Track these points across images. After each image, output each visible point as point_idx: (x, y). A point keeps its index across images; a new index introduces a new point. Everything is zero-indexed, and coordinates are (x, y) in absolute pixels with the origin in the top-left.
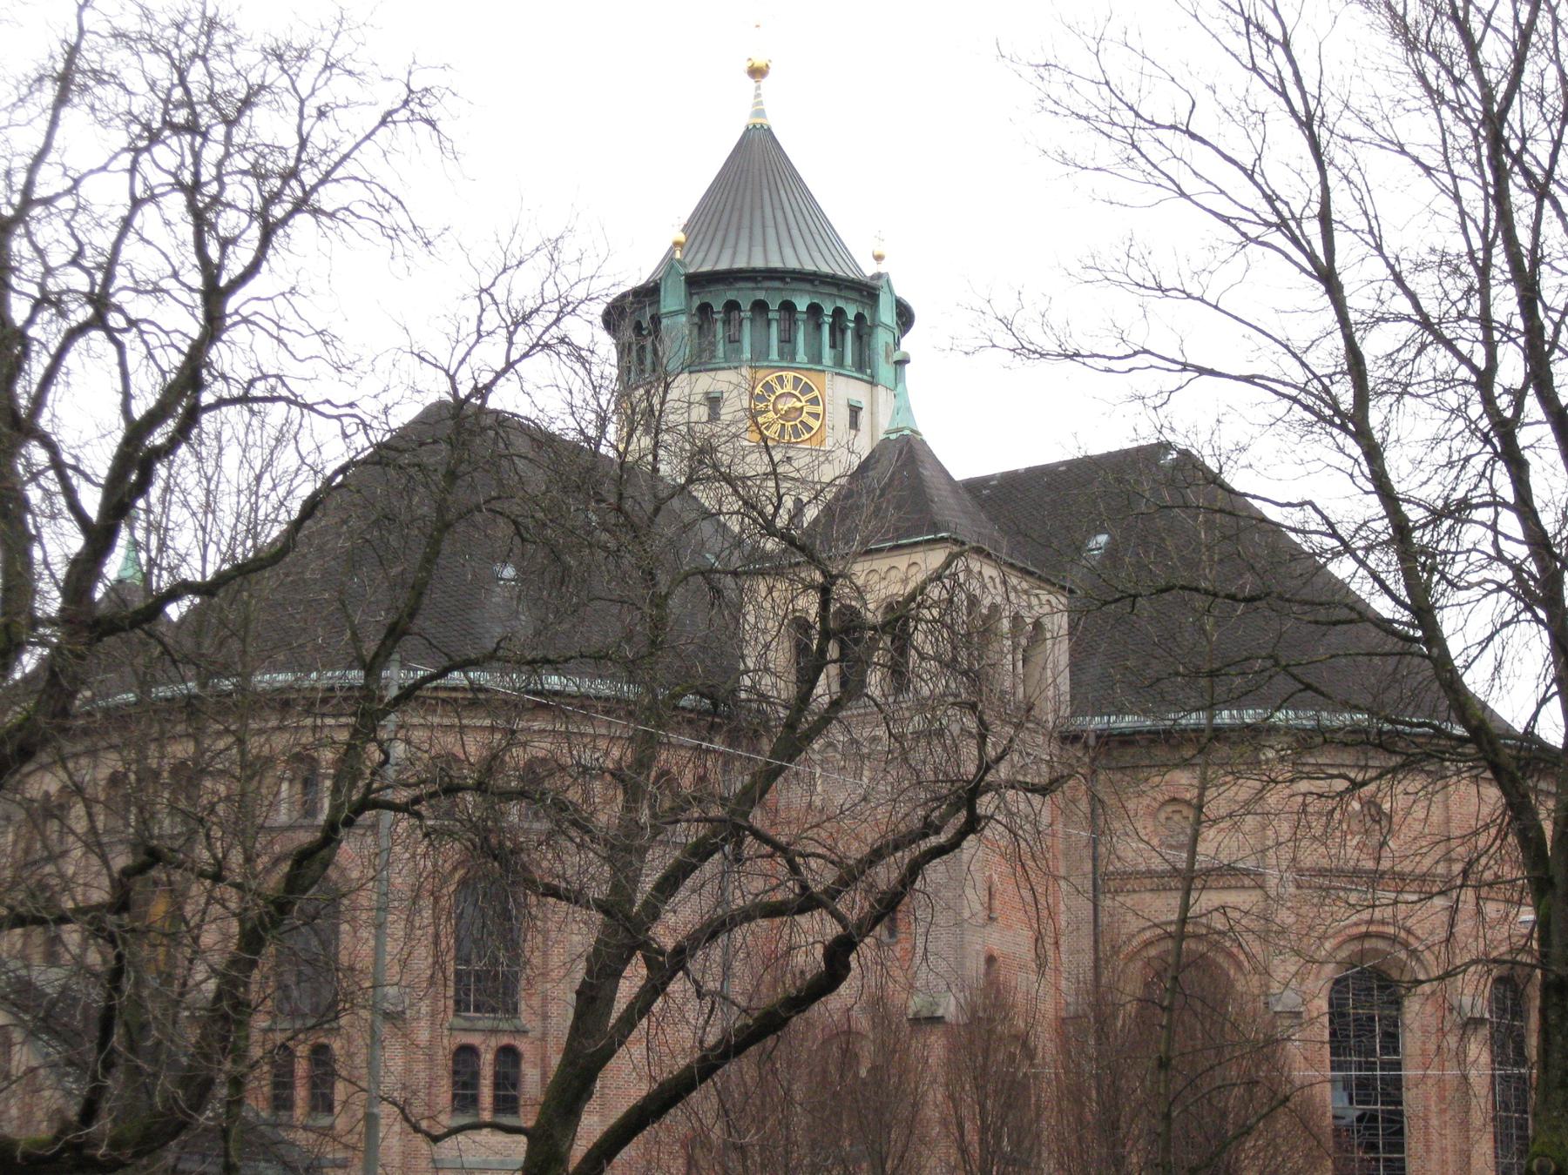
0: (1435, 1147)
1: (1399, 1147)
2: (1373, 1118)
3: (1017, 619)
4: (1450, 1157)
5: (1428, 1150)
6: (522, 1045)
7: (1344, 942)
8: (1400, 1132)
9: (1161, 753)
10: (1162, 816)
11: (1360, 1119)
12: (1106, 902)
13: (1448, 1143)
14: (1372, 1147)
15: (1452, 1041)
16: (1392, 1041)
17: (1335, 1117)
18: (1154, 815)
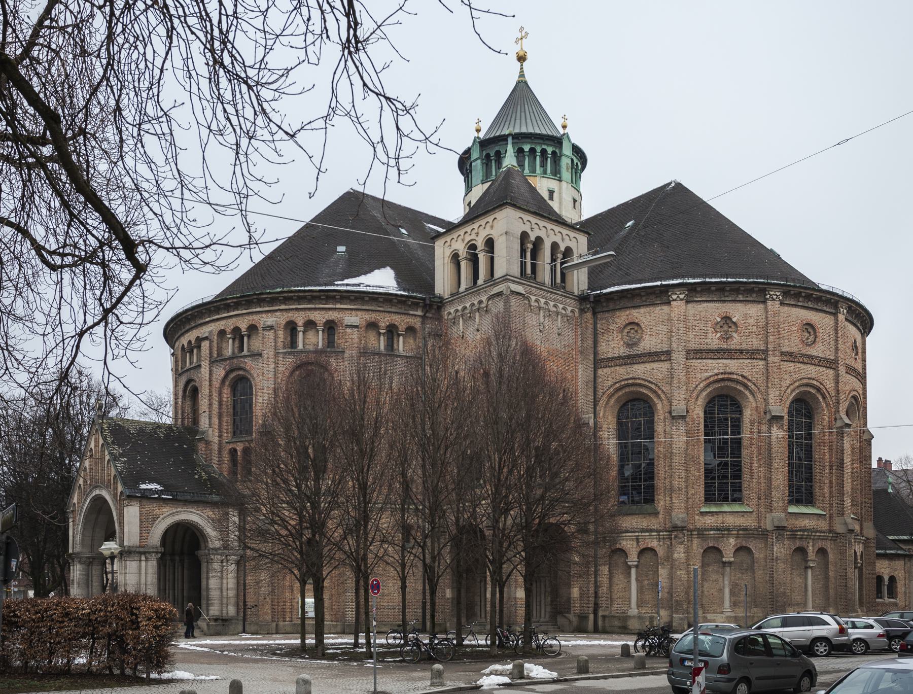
0: (756, 476)
1: (739, 477)
2: (726, 464)
3: (555, 246)
4: (762, 481)
5: (752, 478)
7: (710, 383)
8: (740, 470)
9: (623, 303)
10: (626, 331)
11: (719, 465)
12: (600, 372)
13: (761, 474)
14: (726, 477)
15: (764, 428)
16: (737, 429)
17: (705, 464)
18: (621, 330)
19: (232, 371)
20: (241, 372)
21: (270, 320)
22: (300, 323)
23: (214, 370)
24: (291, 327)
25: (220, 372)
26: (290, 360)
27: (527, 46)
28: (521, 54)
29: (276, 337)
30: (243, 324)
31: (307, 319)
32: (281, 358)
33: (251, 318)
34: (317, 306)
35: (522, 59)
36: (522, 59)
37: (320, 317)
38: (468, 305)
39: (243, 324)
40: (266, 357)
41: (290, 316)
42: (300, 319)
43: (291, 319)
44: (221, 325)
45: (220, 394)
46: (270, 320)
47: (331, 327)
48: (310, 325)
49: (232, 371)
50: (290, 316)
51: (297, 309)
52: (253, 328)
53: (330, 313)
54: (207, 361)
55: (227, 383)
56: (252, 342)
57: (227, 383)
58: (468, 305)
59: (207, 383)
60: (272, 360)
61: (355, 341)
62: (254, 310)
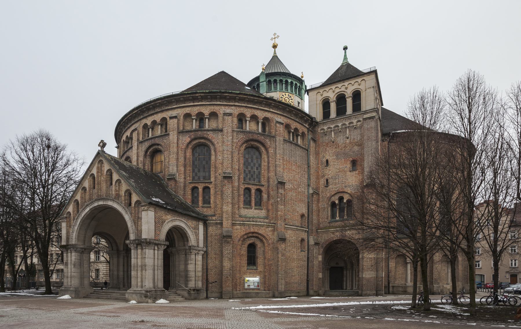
6: (263, 189)
19: (195, 139)
20: (202, 141)
21: (228, 110)
22: (249, 116)
23: (181, 137)
24: (241, 118)
25: (186, 139)
26: (241, 136)
27: (277, 41)
28: (276, 44)
29: (232, 121)
30: (206, 111)
31: (252, 114)
32: (235, 134)
33: (212, 107)
34: (259, 108)
35: (275, 47)
36: (275, 47)
37: (261, 115)
38: (340, 125)
39: (206, 111)
40: (226, 131)
41: (242, 110)
42: (248, 113)
43: (242, 112)
44: (187, 110)
45: (185, 153)
46: (228, 110)
47: (266, 121)
48: (254, 118)
49: (195, 139)
50: (242, 110)
51: (246, 107)
52: (214, 115)
53: (267, 113)
54: (176, 132)
55: (190, 146)
56: (211, 123)
57: (190, 146)
58: (340, 125)
59: (175, 145)
60: (230, 134)
61: (282, 132)
62: (216, 103)
